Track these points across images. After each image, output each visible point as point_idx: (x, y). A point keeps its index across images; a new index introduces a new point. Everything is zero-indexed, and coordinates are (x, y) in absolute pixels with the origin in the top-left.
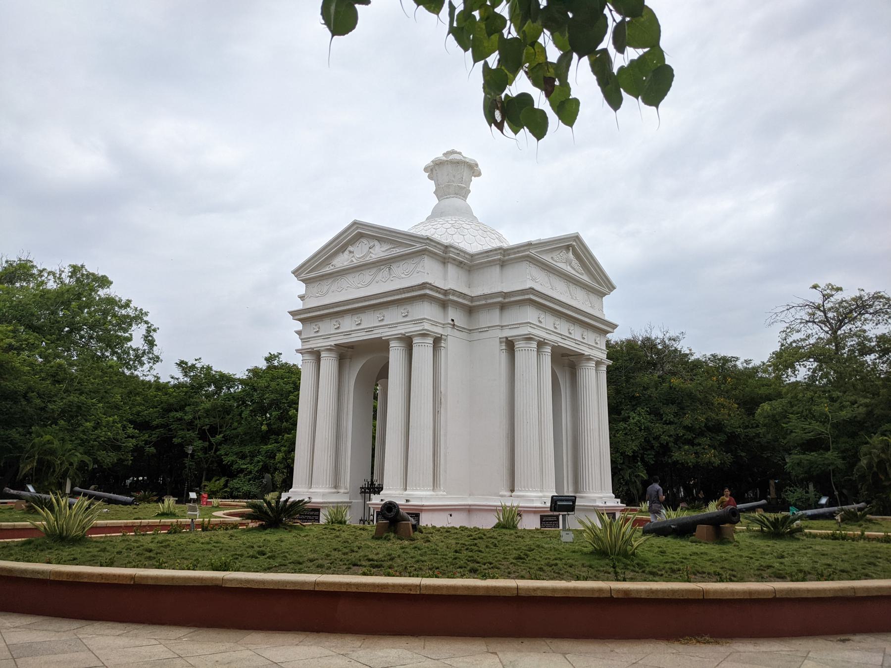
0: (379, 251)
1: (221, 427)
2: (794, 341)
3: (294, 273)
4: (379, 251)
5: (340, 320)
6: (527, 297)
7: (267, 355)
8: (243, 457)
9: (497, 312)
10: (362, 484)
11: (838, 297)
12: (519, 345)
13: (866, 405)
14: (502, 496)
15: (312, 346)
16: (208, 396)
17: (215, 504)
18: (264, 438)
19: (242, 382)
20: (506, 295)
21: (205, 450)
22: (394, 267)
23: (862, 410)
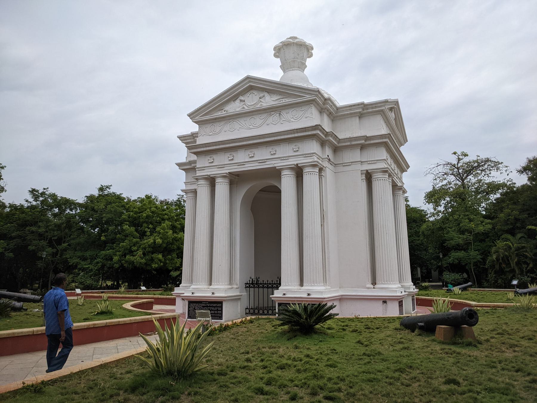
0: (269, 101)
1: (65, 237)
2: (443, 185)
3: (189, 115)
4: (269, 101)
5: (234, 154)
6: (385, 140)
7: (99, 186)
8: (84, 259)
9: (358, 151)
10: (247, 280)
11: (466, 160)
12: (375, 176)
13: (489, 223)
14: (368, 288)
15: (209, 174)
16: (55, 215)
17: (105, 298)
18: (103, 246)
19: (80, 205)
20: (367, 138)
21: (54, 255)
22: (284, 113)
23: (490, 226)
